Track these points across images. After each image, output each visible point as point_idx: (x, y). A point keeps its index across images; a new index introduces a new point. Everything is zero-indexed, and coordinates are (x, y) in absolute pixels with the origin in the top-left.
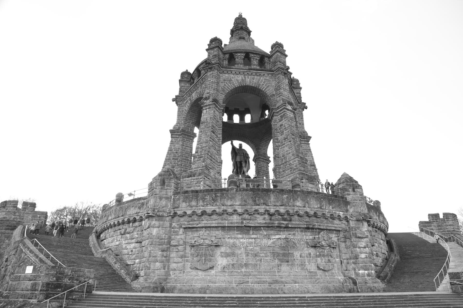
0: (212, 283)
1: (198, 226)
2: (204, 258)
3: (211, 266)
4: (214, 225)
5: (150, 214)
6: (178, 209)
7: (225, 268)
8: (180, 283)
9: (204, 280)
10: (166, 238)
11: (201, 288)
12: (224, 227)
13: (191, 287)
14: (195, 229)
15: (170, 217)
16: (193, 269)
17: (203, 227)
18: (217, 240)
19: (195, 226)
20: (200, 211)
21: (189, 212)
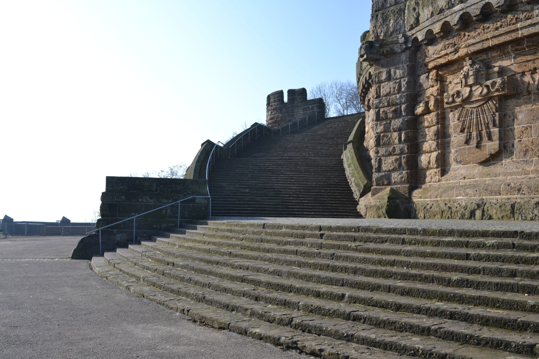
0: (491, 193)
1: (456, 56)
2: (474, 134)
3: (493, 152)
4: (490, 43)
5: (365, 57)
6: (418, 28)
7: (530, 153)
8: (430, 197)
9: (475, 186)
10: (403, 100)
11: (465, 208)
12: (517, 41)
13: (449, 205)
14: (456, 67)
15: (408, 52)
16: (460, 162)
17: (467, 55)
18: (499, 81)
19: (452, 57)
20: (456, 18)
21: (436, 28)
